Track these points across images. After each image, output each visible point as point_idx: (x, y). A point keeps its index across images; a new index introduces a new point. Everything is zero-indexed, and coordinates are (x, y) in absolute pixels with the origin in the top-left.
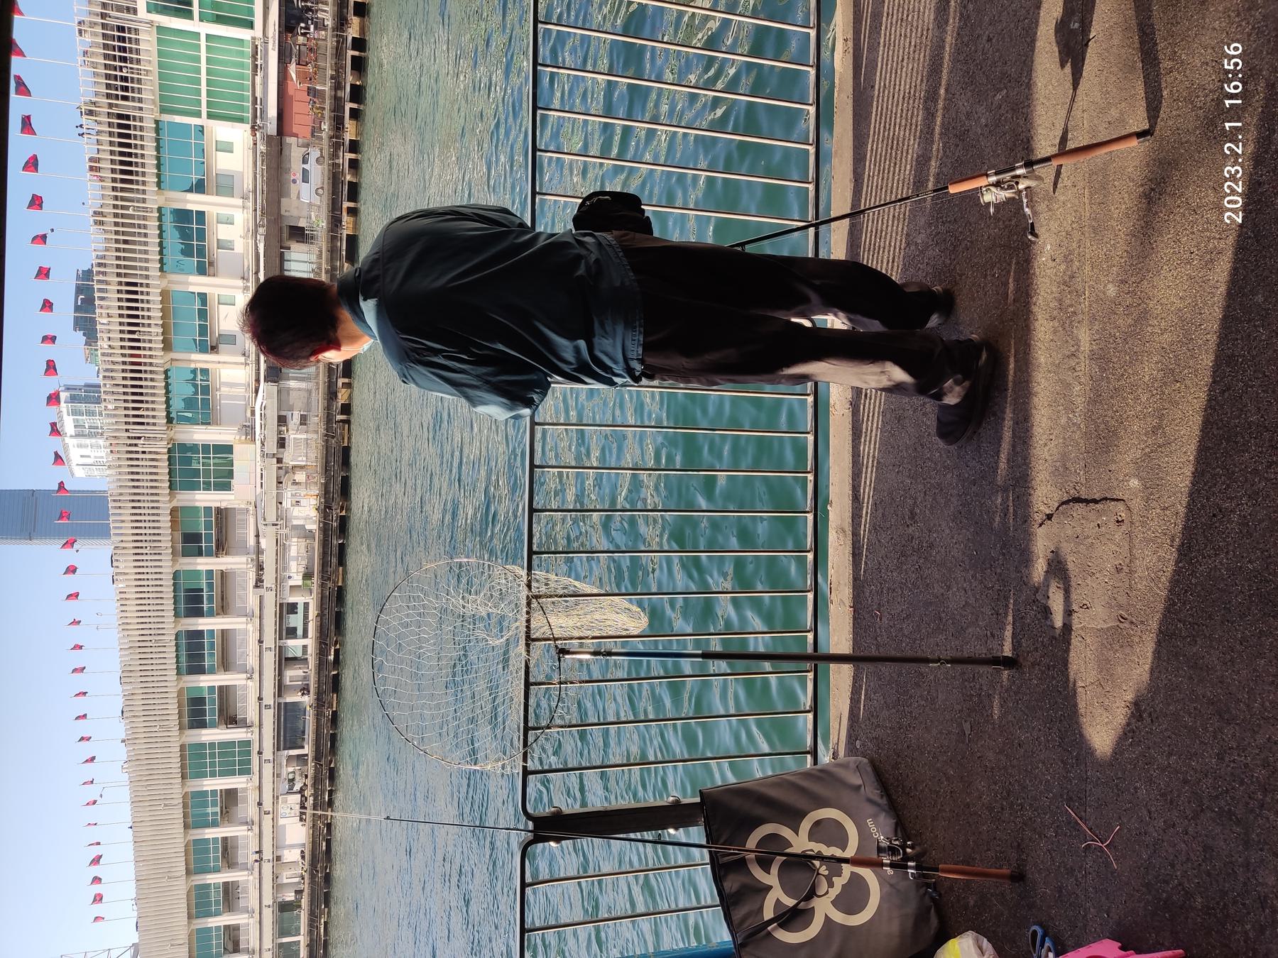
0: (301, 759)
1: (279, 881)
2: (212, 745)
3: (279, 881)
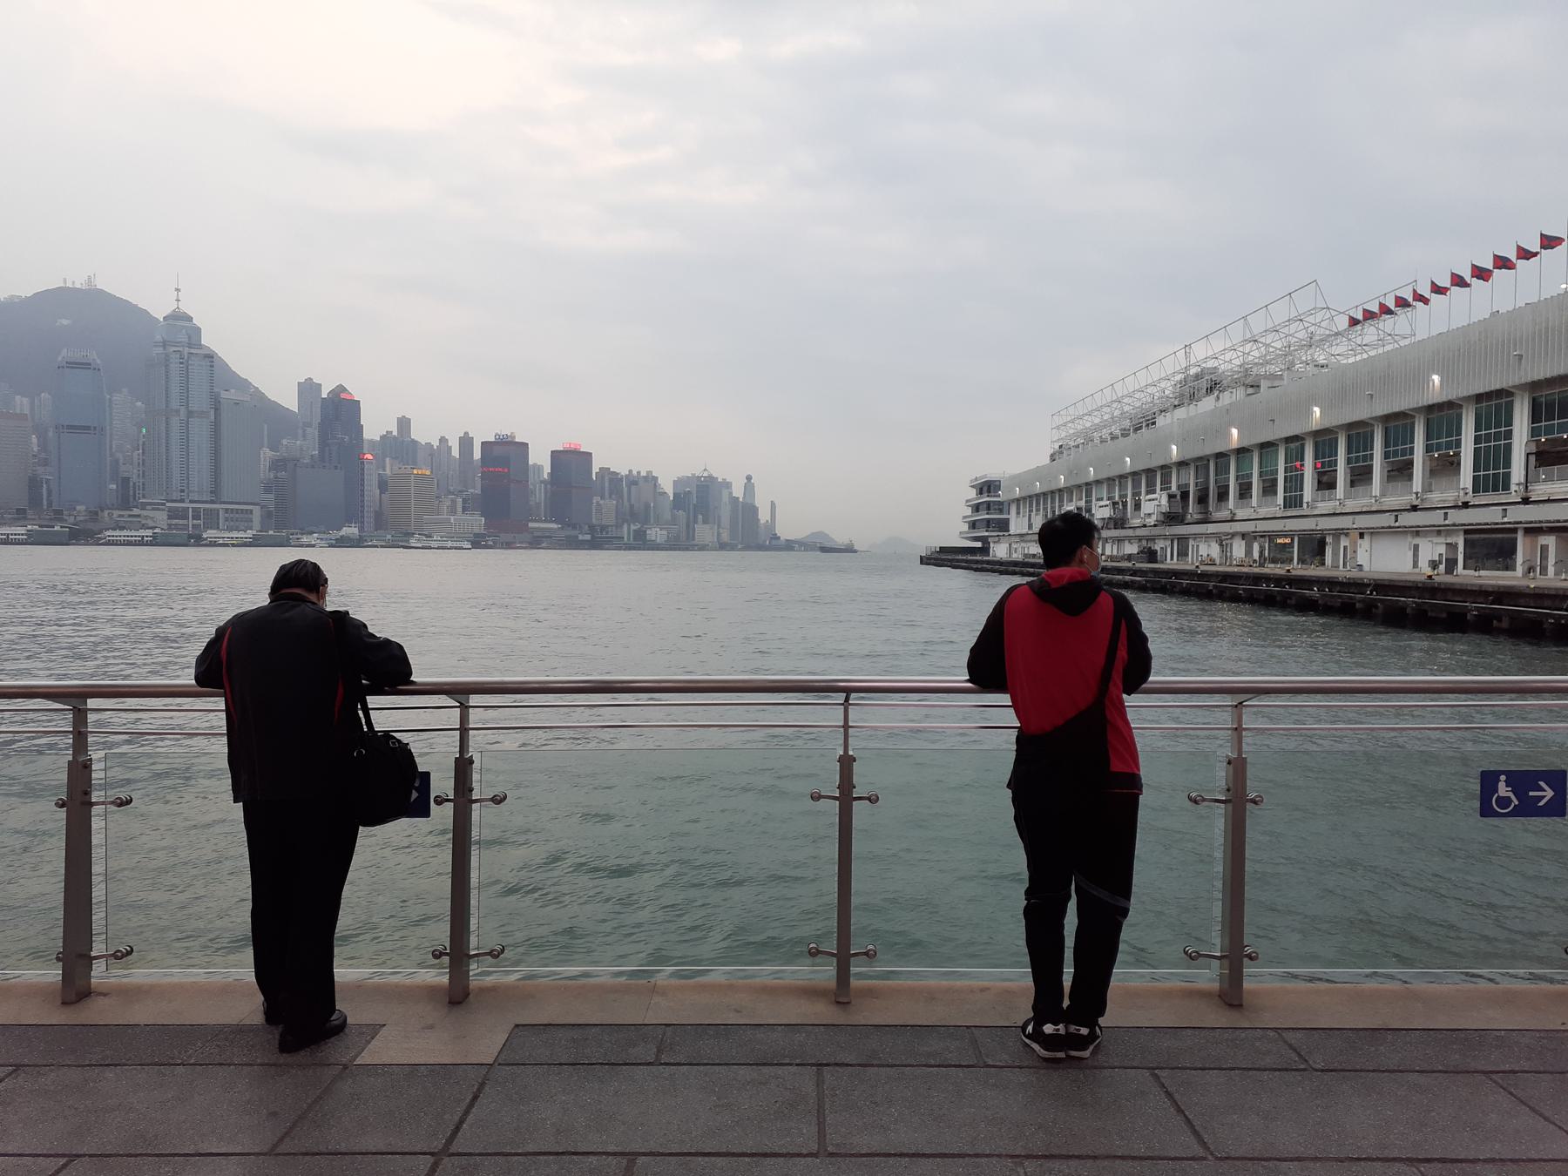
0: (1451, 564)
1: (1342, 537)
2: (1509, 435)
3: (1342, 537)
